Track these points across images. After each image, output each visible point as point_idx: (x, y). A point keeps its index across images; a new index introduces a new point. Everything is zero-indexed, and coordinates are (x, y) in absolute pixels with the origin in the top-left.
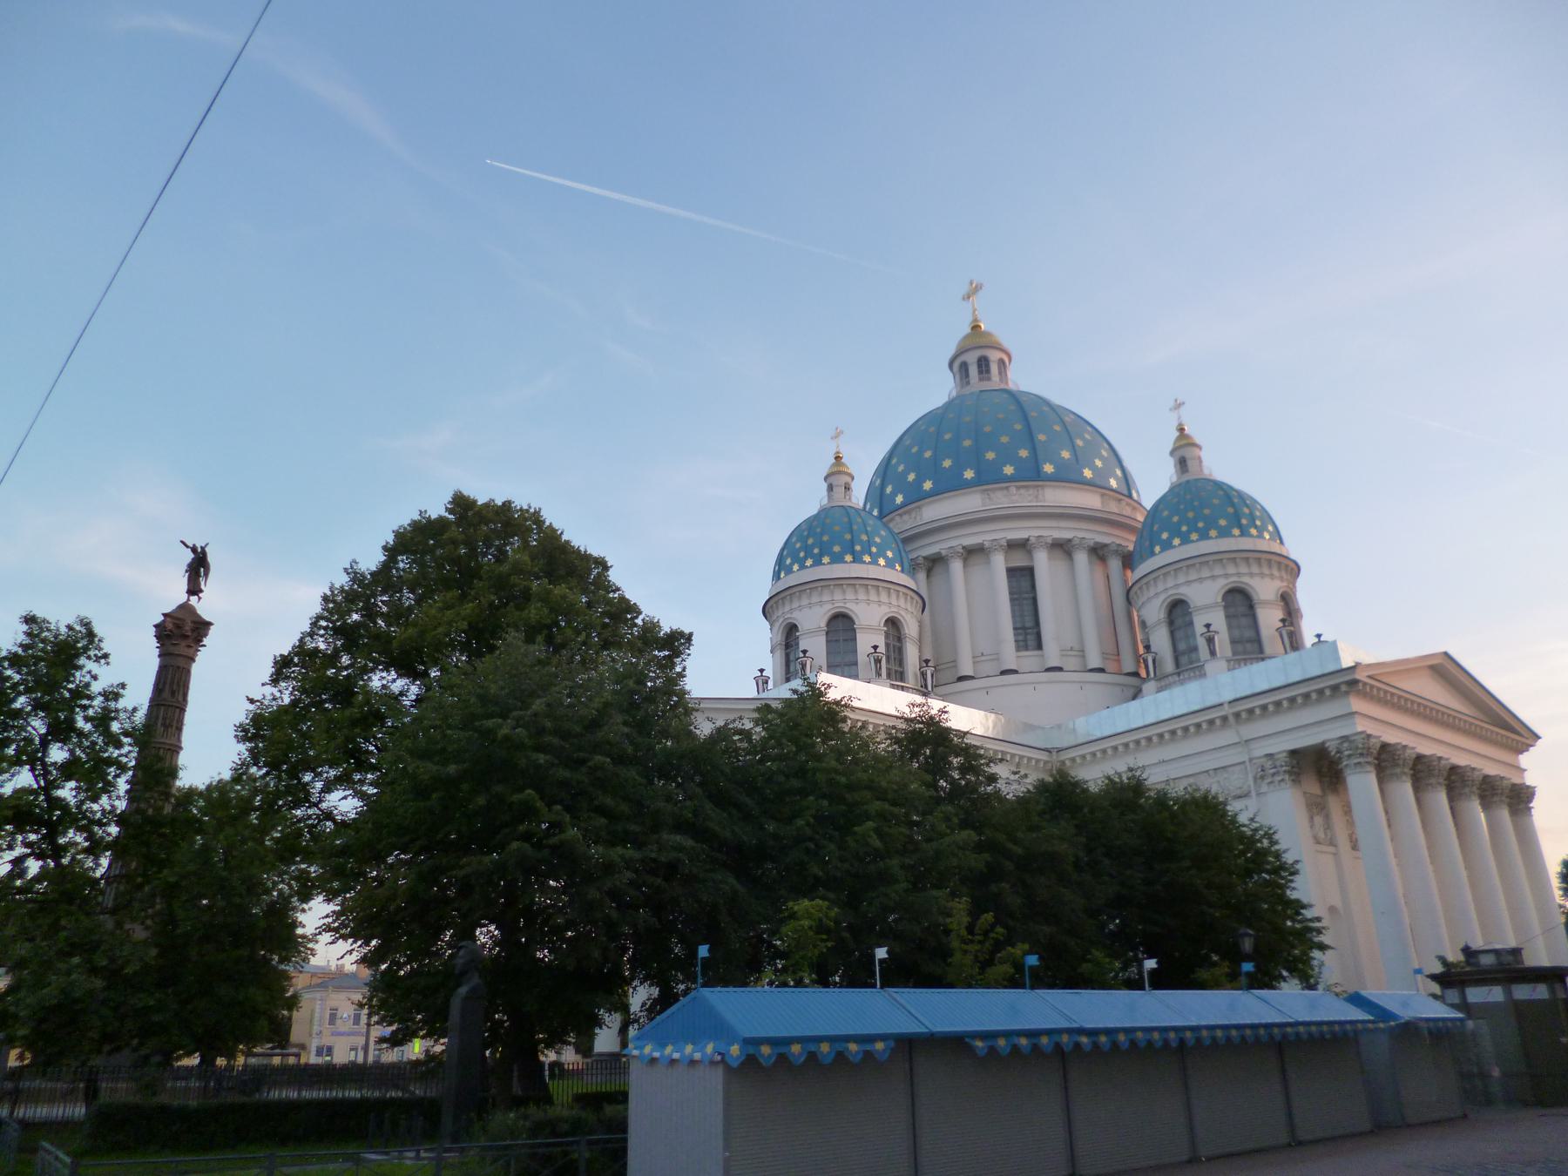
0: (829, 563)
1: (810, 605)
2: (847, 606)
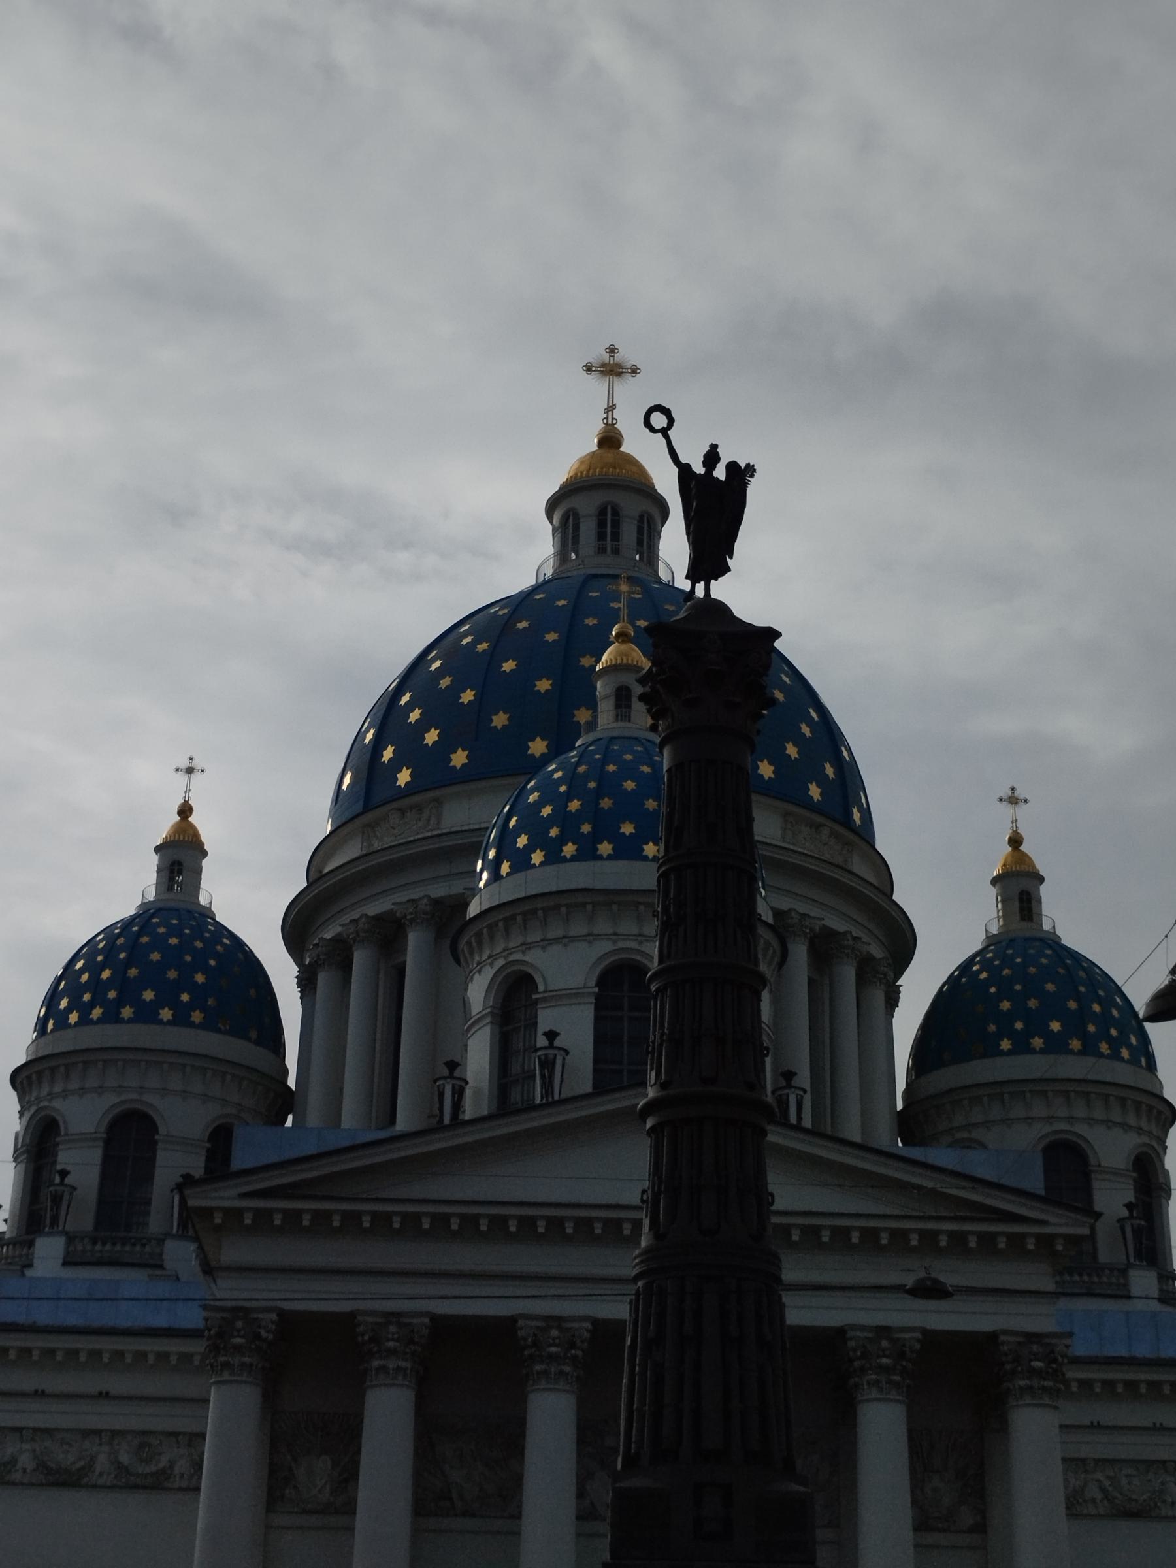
0: (610, 857)
1: (565, 940)
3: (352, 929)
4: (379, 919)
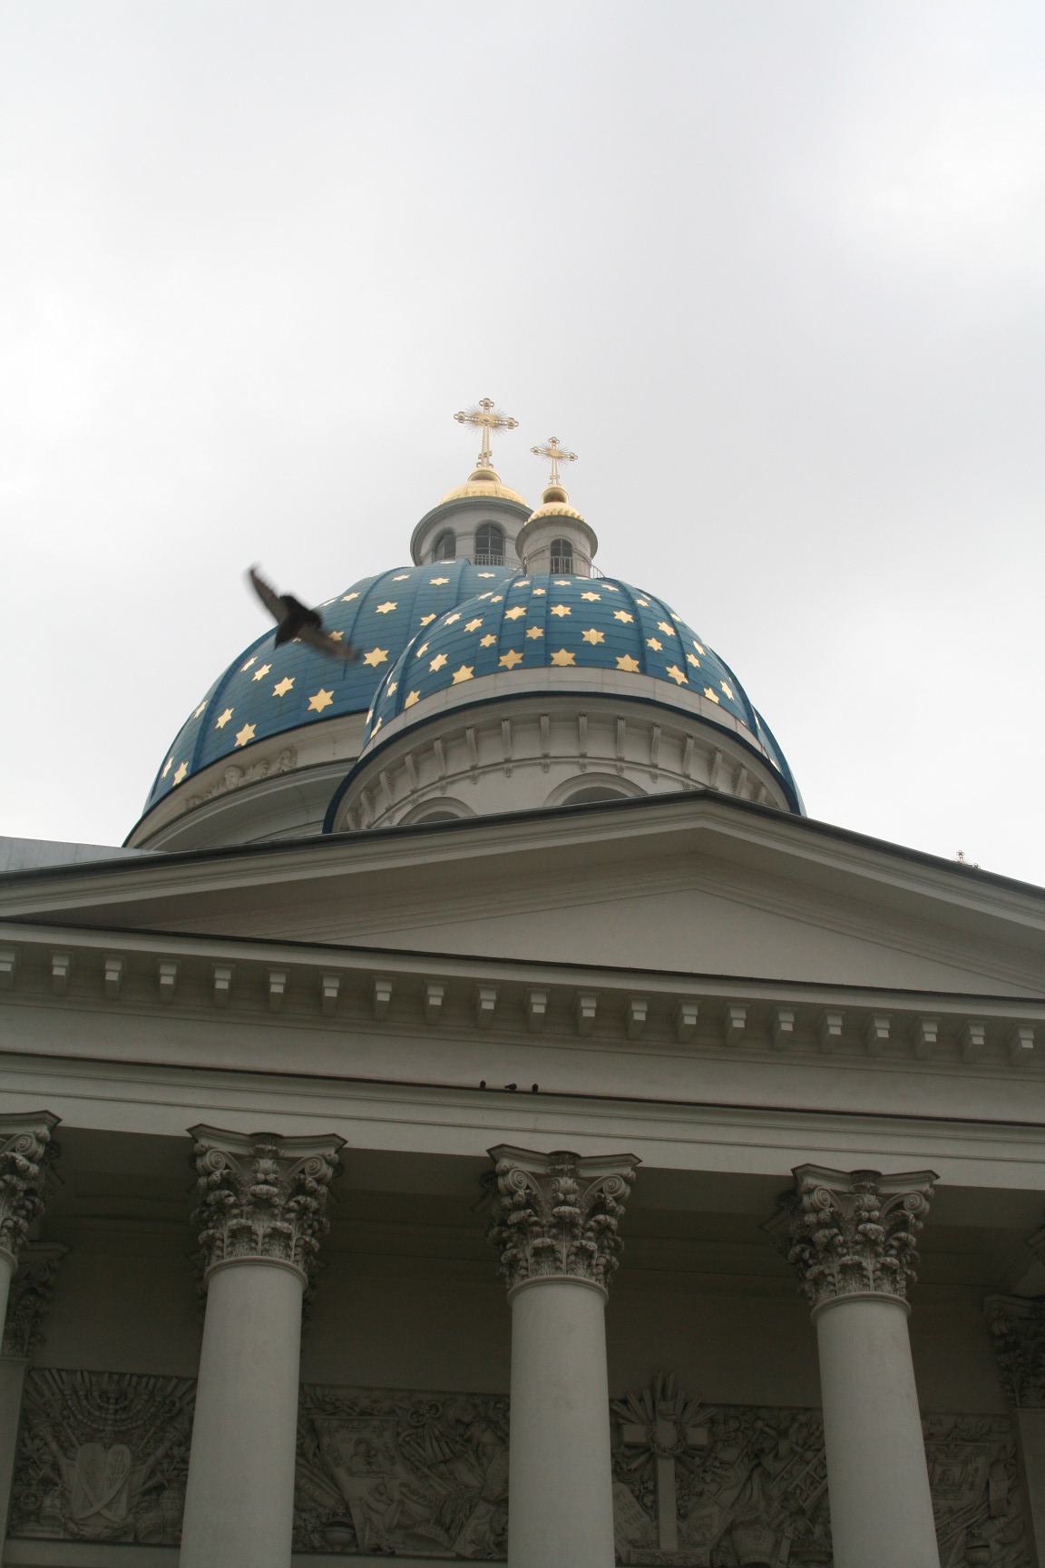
2: (627, 775)
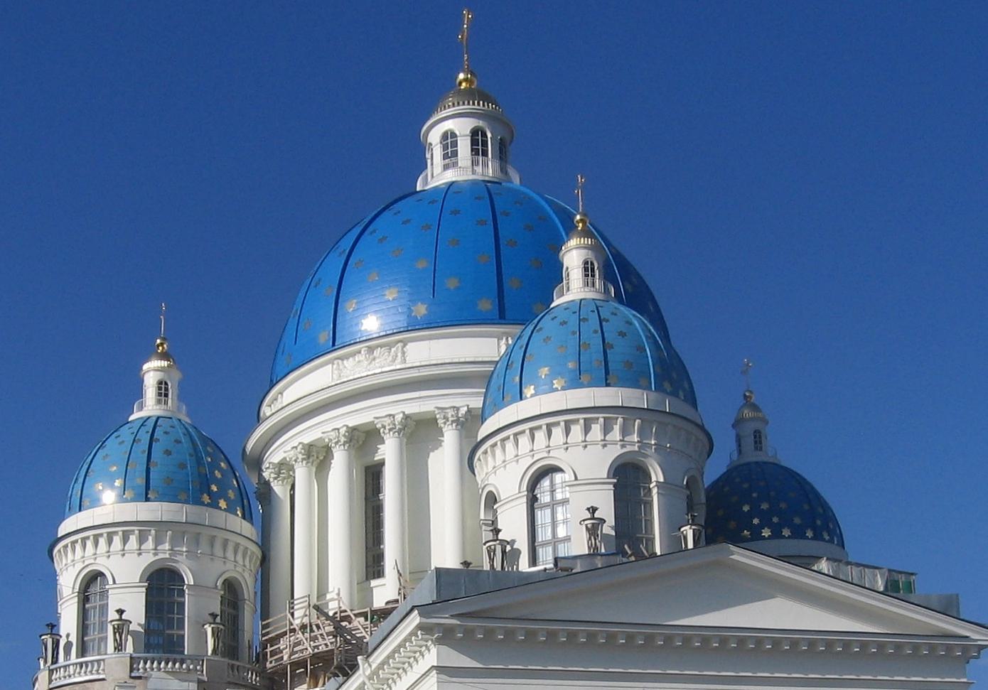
3: (333, 434)
4: (353, 431)
